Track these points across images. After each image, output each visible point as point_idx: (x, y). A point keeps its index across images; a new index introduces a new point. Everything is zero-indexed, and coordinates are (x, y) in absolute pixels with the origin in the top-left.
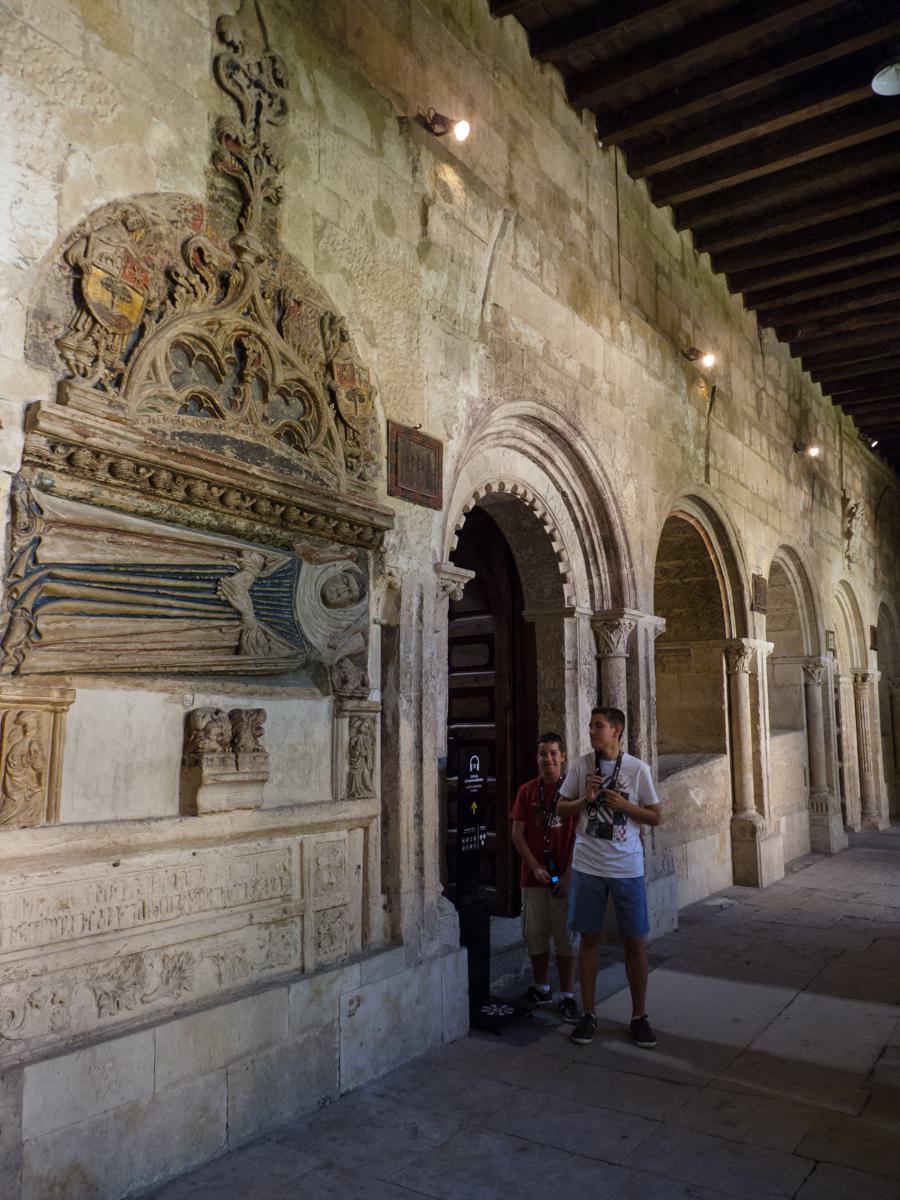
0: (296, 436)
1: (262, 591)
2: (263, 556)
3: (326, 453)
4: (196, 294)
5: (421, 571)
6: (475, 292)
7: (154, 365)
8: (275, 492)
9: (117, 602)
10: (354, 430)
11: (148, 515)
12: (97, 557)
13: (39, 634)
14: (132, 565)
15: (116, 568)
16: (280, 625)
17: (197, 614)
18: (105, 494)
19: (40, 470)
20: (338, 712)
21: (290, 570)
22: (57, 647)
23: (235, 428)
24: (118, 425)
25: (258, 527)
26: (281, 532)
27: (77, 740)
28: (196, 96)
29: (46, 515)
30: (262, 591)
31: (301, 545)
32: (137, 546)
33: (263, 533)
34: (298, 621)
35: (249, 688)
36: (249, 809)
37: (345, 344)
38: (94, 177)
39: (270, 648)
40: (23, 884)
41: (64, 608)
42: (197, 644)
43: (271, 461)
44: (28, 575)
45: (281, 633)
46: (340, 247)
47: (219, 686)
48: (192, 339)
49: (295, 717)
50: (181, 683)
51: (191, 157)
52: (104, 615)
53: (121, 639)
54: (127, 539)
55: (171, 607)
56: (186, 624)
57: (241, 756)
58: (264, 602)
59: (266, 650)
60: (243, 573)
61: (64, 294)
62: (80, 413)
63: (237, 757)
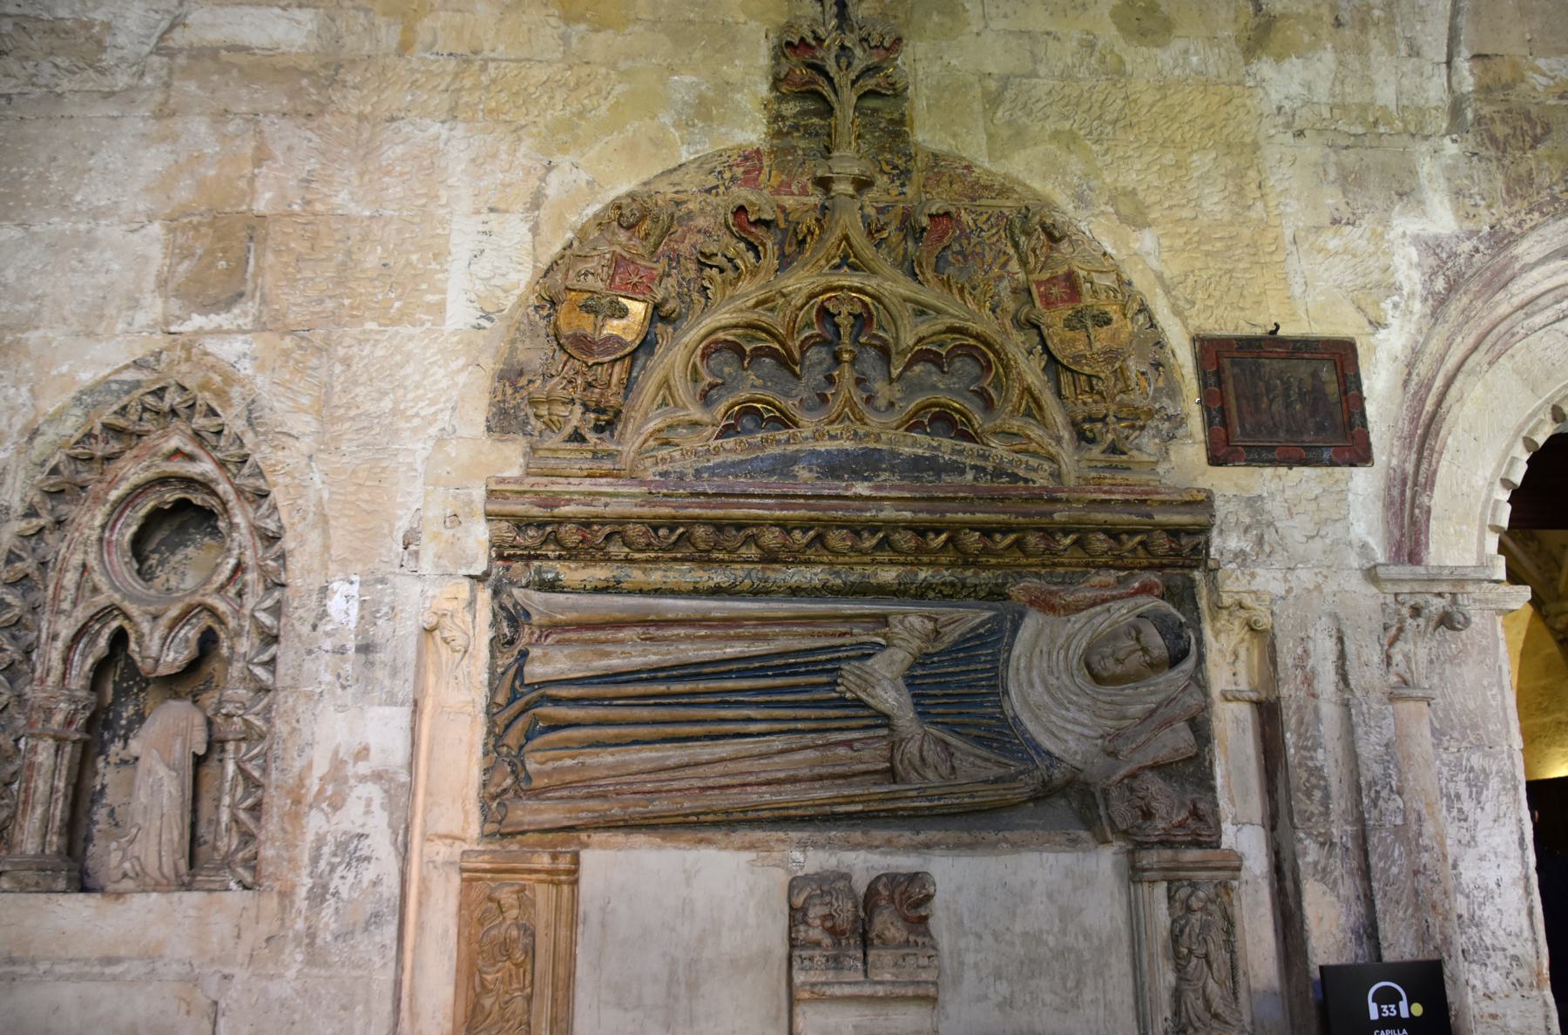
0: (957, 417)
1: (930, 676)
2: (930, 618)
4: (737, 268)
5: (1326, 589)
6: (1418, 55)
7: (666, 383)
8: (908, 515)
9: (654, 722)
10: (1089, 377)
11: (716, 592)
12: (616, 663)
13: (529, 778)
14: (673, 667)
15: (654, 674)
16: (977, 726)
17: (800, 726)
18: (636, 575)
19: (537, 563)
20: (1135, 874)
21: (991, 632)
22: (558, 794)
24: (603, 481)
25: (924, 574)
26: (976, 574)
27: (603, 925)
28: (742, 20)
29: (535, 618)
30: (930, 676)
33: (937, 580)
34: (1016, 717)
35: (922, 837)
37: (1064, 246)
38: (583, 184)
39: (953, 768)
41: (569, 739)
42: (804, 772)
43: (892, 469)
44: (510, 702)
45: (979, 740)
46: (1041, 105)
47: (857, 836)
48: (740, 331)
49: (1033, 883)
50: (781, 835)
51: (738, 96)
52: (636, 742)
53: (664, 775)
54: (668, 632)
56: (778, 743)
57: (872, 954)
58: (937, 692)
59: (944, 770)
60: (892, 650)
61: (543, 339)
62: (545, 480)
63: (865, 955)
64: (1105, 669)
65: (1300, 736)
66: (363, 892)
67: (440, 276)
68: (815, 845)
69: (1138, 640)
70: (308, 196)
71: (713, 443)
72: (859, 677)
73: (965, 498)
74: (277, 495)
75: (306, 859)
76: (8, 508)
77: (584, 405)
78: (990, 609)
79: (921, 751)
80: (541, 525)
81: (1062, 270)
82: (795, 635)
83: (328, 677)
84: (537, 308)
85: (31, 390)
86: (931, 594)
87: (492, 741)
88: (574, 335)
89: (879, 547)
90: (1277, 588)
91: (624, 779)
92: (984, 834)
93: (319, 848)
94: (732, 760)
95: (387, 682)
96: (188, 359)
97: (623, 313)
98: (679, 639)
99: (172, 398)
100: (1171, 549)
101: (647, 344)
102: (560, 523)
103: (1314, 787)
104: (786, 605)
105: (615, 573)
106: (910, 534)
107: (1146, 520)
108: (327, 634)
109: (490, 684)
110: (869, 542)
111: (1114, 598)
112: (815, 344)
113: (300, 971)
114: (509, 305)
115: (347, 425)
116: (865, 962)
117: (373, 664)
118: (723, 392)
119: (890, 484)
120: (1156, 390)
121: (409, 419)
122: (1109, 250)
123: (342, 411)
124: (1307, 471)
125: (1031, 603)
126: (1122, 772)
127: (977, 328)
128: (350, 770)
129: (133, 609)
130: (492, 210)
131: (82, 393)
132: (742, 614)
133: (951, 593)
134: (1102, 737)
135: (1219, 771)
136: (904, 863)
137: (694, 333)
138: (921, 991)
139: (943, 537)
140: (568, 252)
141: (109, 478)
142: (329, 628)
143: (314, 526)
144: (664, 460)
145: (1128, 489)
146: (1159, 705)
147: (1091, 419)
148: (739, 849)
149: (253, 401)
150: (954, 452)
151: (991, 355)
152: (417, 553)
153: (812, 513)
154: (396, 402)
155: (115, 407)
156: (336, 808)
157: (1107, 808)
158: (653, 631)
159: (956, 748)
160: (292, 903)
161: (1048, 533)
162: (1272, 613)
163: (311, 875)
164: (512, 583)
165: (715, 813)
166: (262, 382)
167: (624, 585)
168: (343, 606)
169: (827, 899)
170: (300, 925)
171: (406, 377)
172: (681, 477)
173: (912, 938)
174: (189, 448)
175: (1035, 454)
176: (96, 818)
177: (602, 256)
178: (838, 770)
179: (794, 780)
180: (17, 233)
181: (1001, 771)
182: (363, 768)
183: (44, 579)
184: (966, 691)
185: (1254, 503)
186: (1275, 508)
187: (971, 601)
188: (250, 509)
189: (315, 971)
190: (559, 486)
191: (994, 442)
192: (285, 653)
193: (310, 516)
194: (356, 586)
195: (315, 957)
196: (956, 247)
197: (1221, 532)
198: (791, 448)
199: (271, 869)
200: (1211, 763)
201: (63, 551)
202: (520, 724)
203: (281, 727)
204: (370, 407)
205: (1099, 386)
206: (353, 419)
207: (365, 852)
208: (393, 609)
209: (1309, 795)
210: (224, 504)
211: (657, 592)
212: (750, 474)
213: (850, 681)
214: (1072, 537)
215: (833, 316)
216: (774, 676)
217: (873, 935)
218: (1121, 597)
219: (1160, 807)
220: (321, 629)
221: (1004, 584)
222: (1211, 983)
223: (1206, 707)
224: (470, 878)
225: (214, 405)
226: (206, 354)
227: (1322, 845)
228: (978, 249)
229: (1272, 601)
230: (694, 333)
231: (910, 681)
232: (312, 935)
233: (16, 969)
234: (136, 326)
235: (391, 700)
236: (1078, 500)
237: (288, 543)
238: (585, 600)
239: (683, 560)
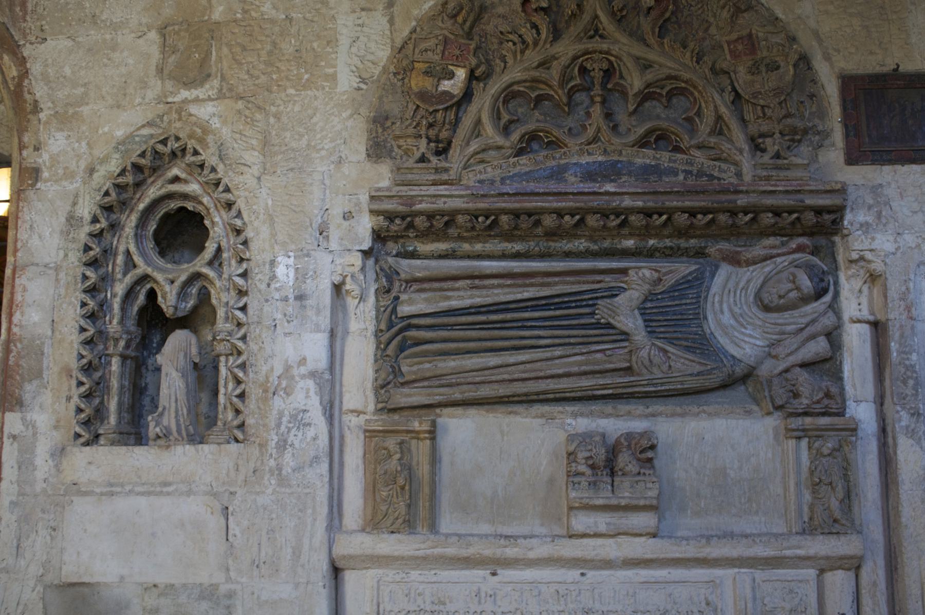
2: (656, 271)
3: (715, 143)
4: (524, 42)
8: (640, 204)
9: (480, 340)
10: (763, 107)
11: (517, 256)
12: (455, 304)
13: (402, 374)
16: (686, 339)
17: (572, 340)
19: (402, 241)
21: (696, 279)
23: (581, 152)
29: (403, 276)
31: (713, 249)
32: (499, 286)
33: (661, 245)
36: (641, 535)
39: (670, 366)
40: (403, 578)
42: (575, 369)
43: (630, 174)
45: (687, 349)
47: (609, 409)
48: (527, 84)
50: (560, 408)
52: (468, 352)
53: (486, 372)
55: (540, 337)
56: (558, 352)
57: (617, 479)
58: (661, 318)
59: (665, 368)
62: (405, 188)
64: (771, 302)
65: (900, 345)
66: (308, 444)
67: (333, 56)
68: (582, 415)
69: (794, 282)
70: (246, 7)
71: (512, 160)
72: (610, 309)
73: (678, 192)
74: (241, 204)
75: (273, 424)
76: (82, 218)
77: (427, 137)
78: (696, 263)
79: (649, 354)
80: (403, 218)
81: (745, 32)
82: (567, 283)
83: (279, 316)
84: (395, 74)
85: (88, 144)
86: (658, 254)
87: (379, 353)
88: (420, 92)
89: (624, 224)
90: (889, 247)
91: (461, 375)
92: (690, 408)
93: (280, 418)
94: (529, 362)
95: (314, 318)
96: (180, 119)
97: (451, 76)
98: (493, 287)
99: (172, 145)
100: (818, 222)
101: (467, 95)
102: (416, 215)
103: (908, 377)
104: (562, 264)
105: (452, 245)
106: (642, 216)
107: (802, 204)
108: (277, 289)
109: (377, 317)
110: (614, 222)
111: (779, 255)
112: (578, 90)
113: (274, 490)
114: (377, 72)
115: (280, 157)
116: (612, 486)
117: (305, 307)
118: (518, 125)
119: (629, 184)
120: (810, 113)
121: (318, 151)
122: (780, 16)
123: (277, 148)
124: (915, 167)
125: (724, 259)
126: (781, 368)
127: (686, 75)
128: (295, 372)
129: (159, 277)
130: (363, 9)
131: (119, 144)
132: (534, 269)
133: (671, 254)
134: (768, 346)
135: (846, 368)
136: (638, 426)
137: (495, 86)
138: (648, 503)
139: (664, 217)
140: (414, 36)
141: (138, 196)
142: (278, 285)
143: (264, 222)
144: (480, 172)
145: (788, 183)
146: (807, 325)
147: (762, 136)
148: (534, 418)
149: (222, 144)
150: (670, 161)
151: (696, 94)
152: (328, 237)
153: (578, 204)
154: (309, 141)
155: (139, 152)
156: (288, 394)
157: (770, 391)
158: (477, 282)
159: (673, 354)
160: (267, 450)
161: (733, 213)
162: (885, 264)
163: (277, 434)
164: (388, 254)
165: (519, 396)
166: (226, 132)
167: (458, 253)
168: (285, 271)
169: (590, 447)
170: (272, 463)
171: (316, 124)
172: (492, 182)
173: (642, 471)
174: (183, 175)
175: (725, 161)
176: (143, 403)
177: (437, 37)
178: (597, 368)
179: (568, 375)
180: (69, 43)
181: (702, 368)
182: (303, 370)
183: (106, 260)
184: (679, 317)
185: (876, 190)
186: (891, 192)
187: (685, 259)
188: (223, 212)
189: (283, 490)
190: (415, 191)
191: (697, 153)
192: (253, 301)
193: (261, 216)
194: (292, 259)
195: (283, 481)
196: (674, 19)
197: (852, 209)
198: (562, 162)
199: (253, 431)
200: (841, 362)
201: (115, 243)
202: (395, 342)
203: (253, 346)
204: (294, 145)
205: (769, 112)
206: (283, 153)
207: (307, 421)
208: (315, 272)
209: (905, 382)
210: (208, 209)
211: (479, 257)
212: (536, 180)
213: (603, 312)
214: (750, 216)
215: (590, 71)
216: (555, 309)
217: (616, 469)
218: (784, 254)
219: (805, 390)
220: (273, 286)
221: (706, 247)
222: (833, 499)
223: (838, 327)
224: (369, 434)
225: (198, 148)
226: (191, 115)
227: (913, 415)
228: (688, 20)
229: (885, 255)
230: (495, 86)
231: (643, 311)
232: (279, 468)
233: (113, 489)
234: (147, 100)
235: (318, 330)
236: (754, 191)
237: (249, 233)
238: (434, 263)
239: (495, 236)
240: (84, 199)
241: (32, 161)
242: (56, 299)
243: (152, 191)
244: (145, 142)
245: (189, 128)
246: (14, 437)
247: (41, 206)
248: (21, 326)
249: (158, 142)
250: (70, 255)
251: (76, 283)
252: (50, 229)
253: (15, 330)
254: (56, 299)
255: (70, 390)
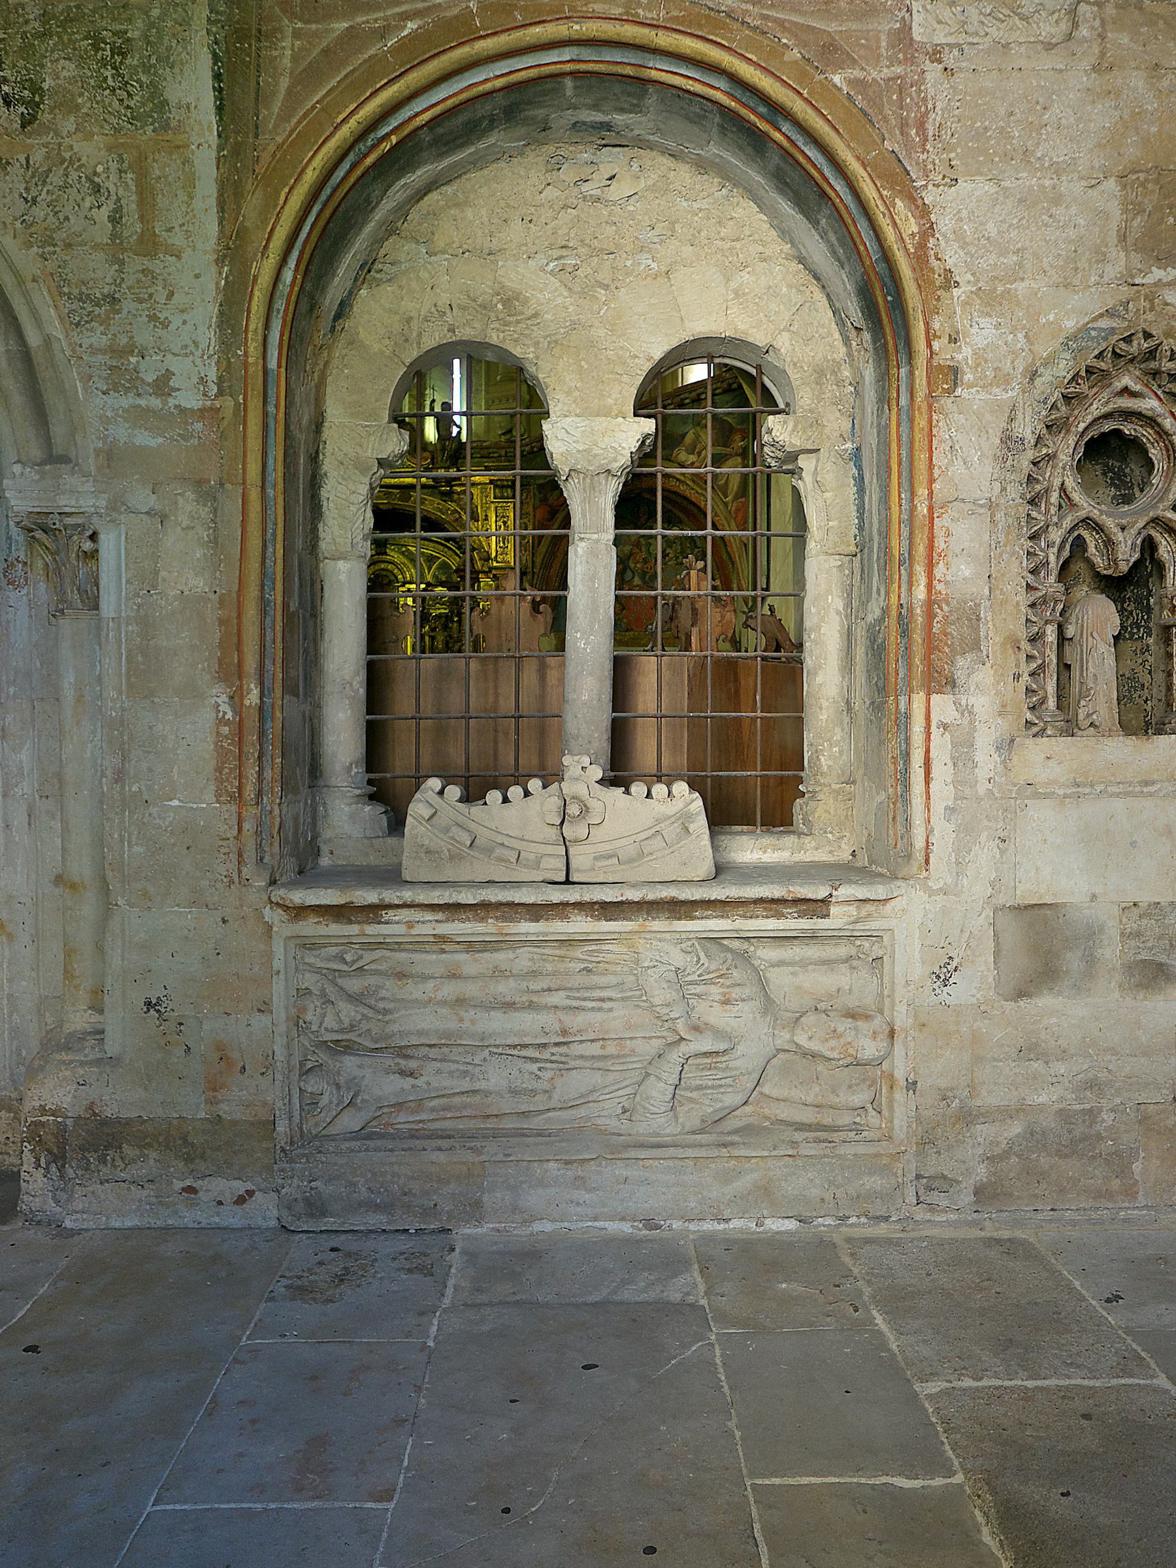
96: (1152, 309)
155: (1096, 352)
174: (1137, 387)
180: (990, 188)
226: (1167, 304)
234: (1106, 279)
240: (1024, 413)
241: (949, 357)
242: (993, 547)
243: (1095, 406)
244: (1105, 339)
245: (1166, 323)
246: (945, 726)
247: (964, 421)
248: (947, 583)
249: (1121, 339)
250: (1008, 488)
251: (1020, 528)
252: (979, 453)
253: (939, 587)
254: (993, 547)
255: (1017, 666)
